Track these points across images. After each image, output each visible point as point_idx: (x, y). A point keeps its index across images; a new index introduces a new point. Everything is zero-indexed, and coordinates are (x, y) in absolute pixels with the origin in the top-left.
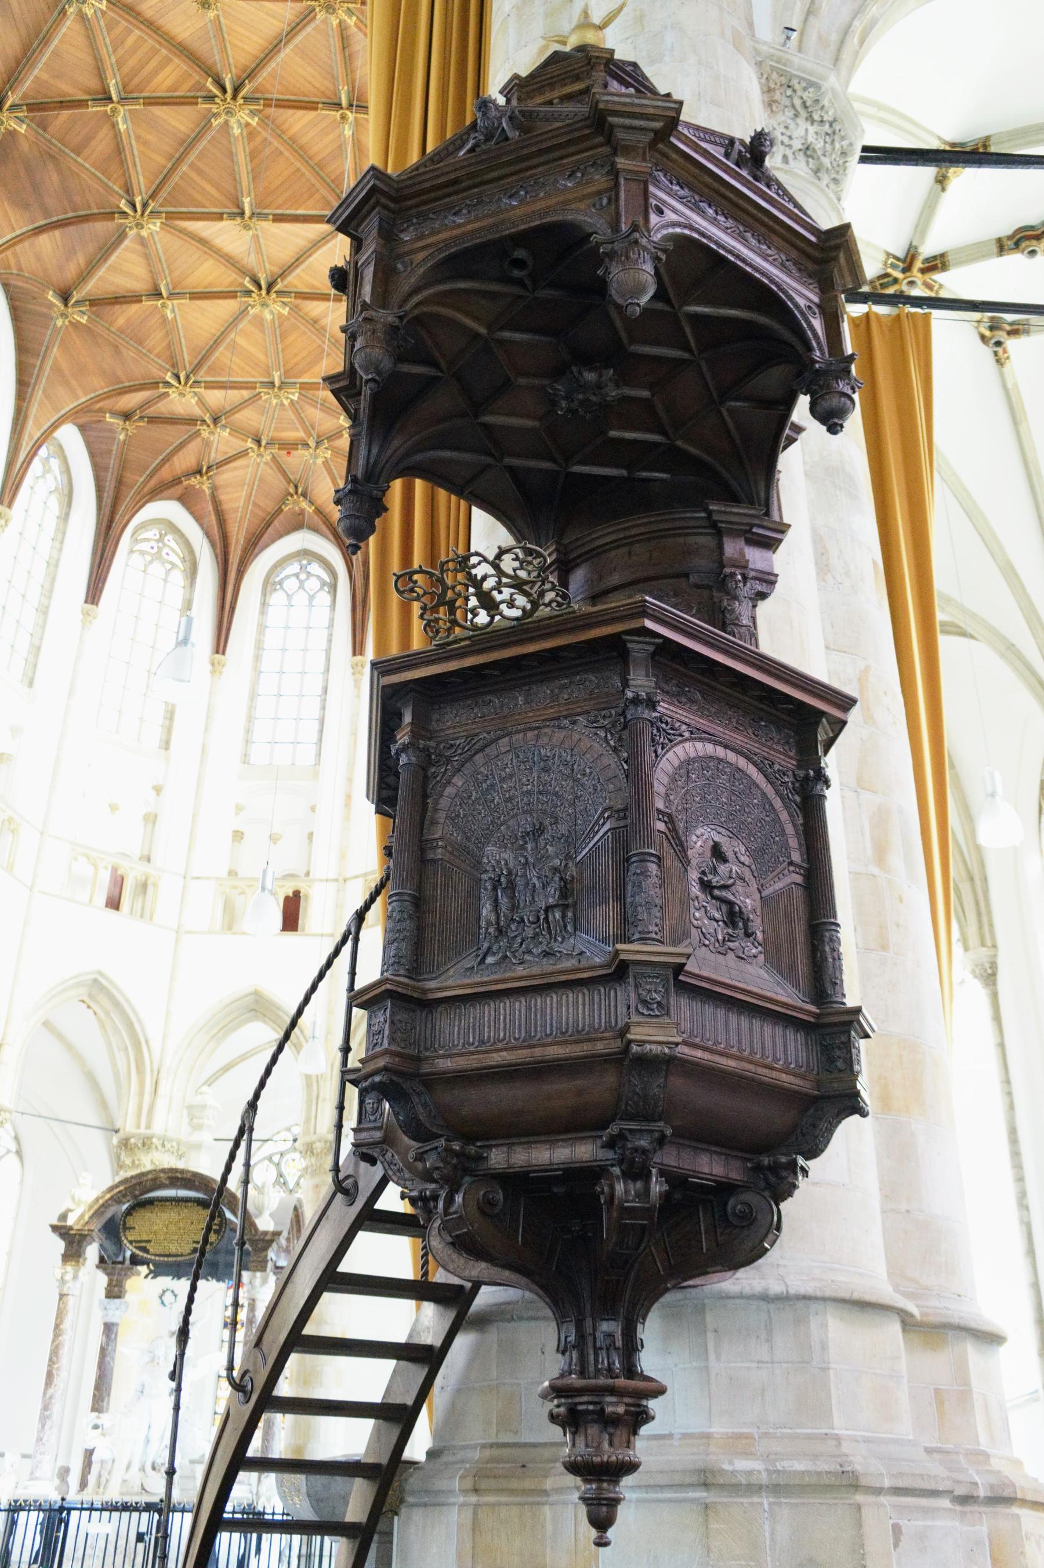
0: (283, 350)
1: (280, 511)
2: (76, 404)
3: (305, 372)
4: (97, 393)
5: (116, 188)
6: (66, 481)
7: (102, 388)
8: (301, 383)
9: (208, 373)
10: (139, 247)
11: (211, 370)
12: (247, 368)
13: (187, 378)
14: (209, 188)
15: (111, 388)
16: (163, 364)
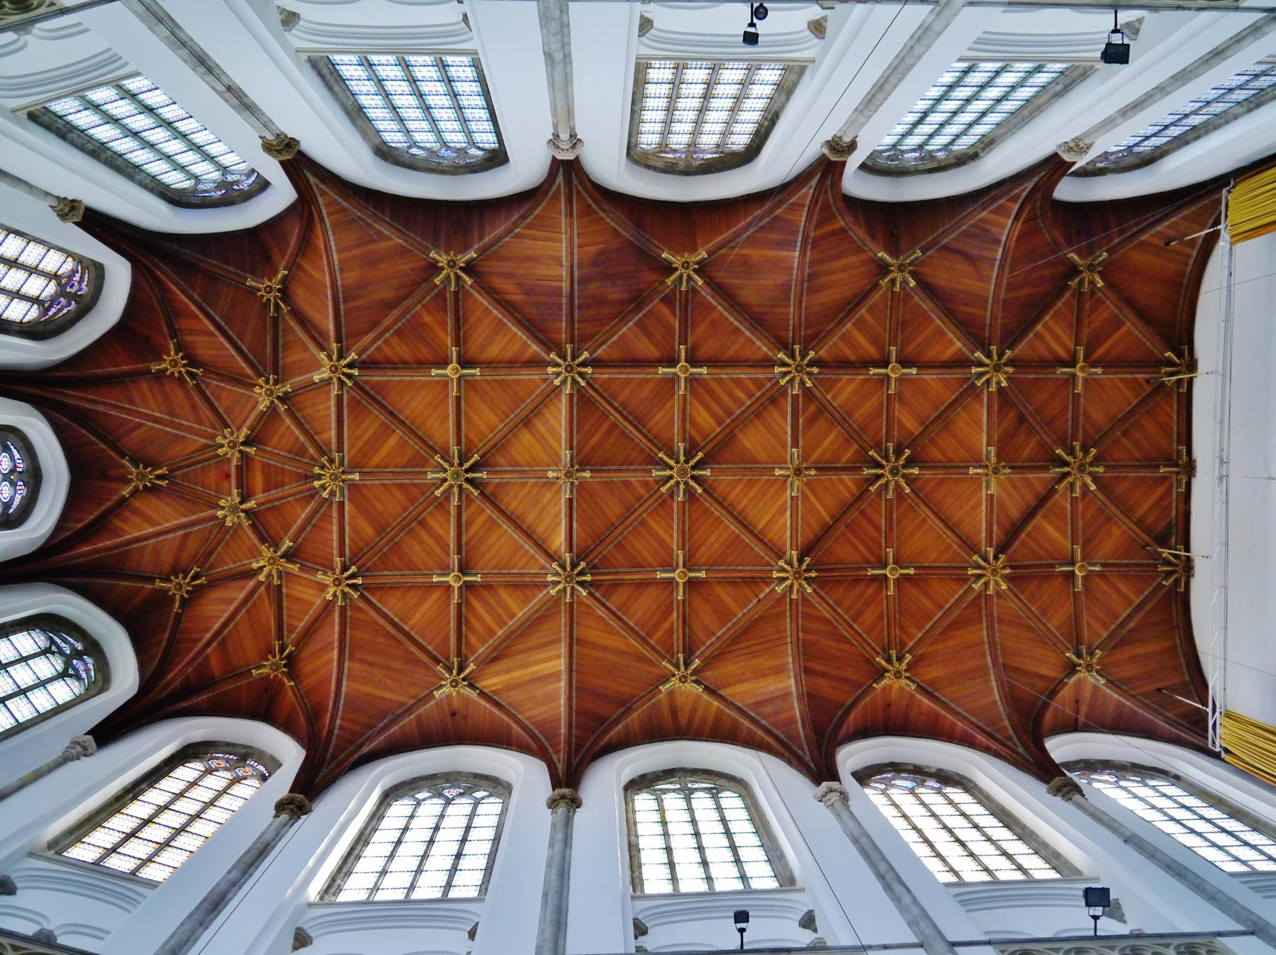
0: (385, 486)
1: (123, 455)
2: (334, 248)
3: (357, 509)
4: (338, 273)
5: (599, 351)
6: (194, 200)
7: (342, 279)
8: (343, 502)
9: (352, 399)
10: (527, 356)
11: (355, 404)
12: (360, 443)
13: (349, 376)
14: (596, 438)
15: (340, 289)
16: (368, 353)
